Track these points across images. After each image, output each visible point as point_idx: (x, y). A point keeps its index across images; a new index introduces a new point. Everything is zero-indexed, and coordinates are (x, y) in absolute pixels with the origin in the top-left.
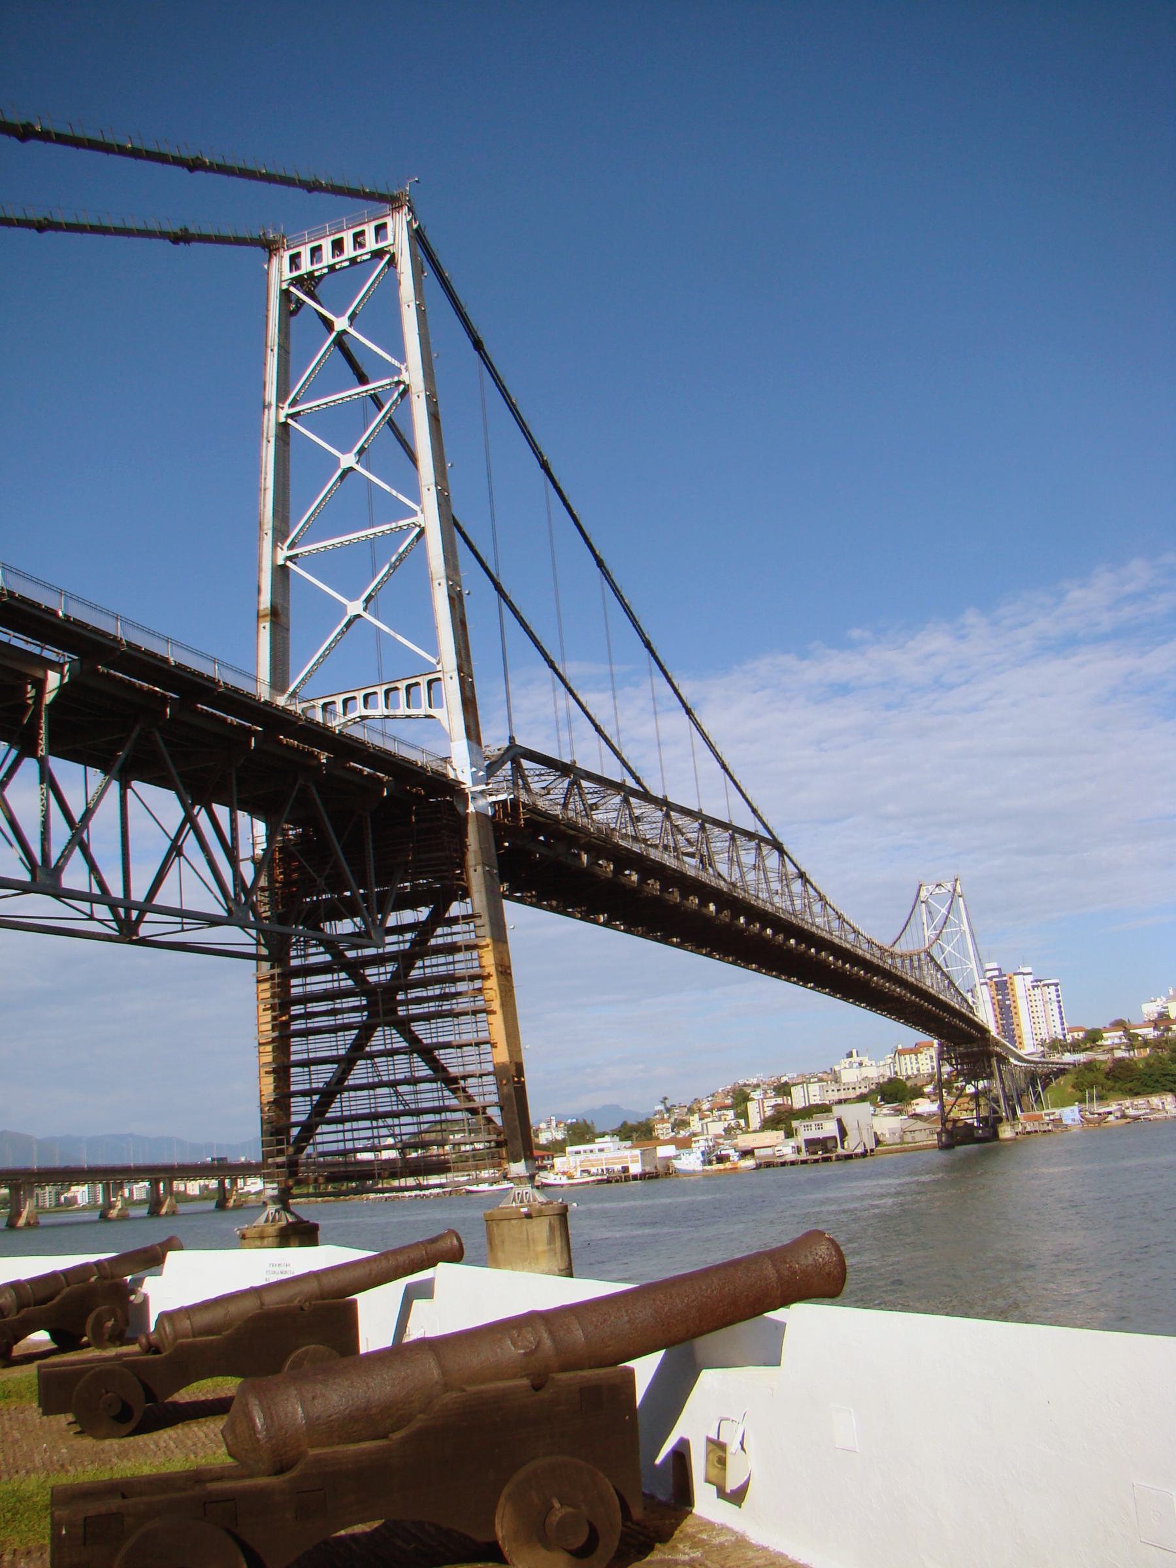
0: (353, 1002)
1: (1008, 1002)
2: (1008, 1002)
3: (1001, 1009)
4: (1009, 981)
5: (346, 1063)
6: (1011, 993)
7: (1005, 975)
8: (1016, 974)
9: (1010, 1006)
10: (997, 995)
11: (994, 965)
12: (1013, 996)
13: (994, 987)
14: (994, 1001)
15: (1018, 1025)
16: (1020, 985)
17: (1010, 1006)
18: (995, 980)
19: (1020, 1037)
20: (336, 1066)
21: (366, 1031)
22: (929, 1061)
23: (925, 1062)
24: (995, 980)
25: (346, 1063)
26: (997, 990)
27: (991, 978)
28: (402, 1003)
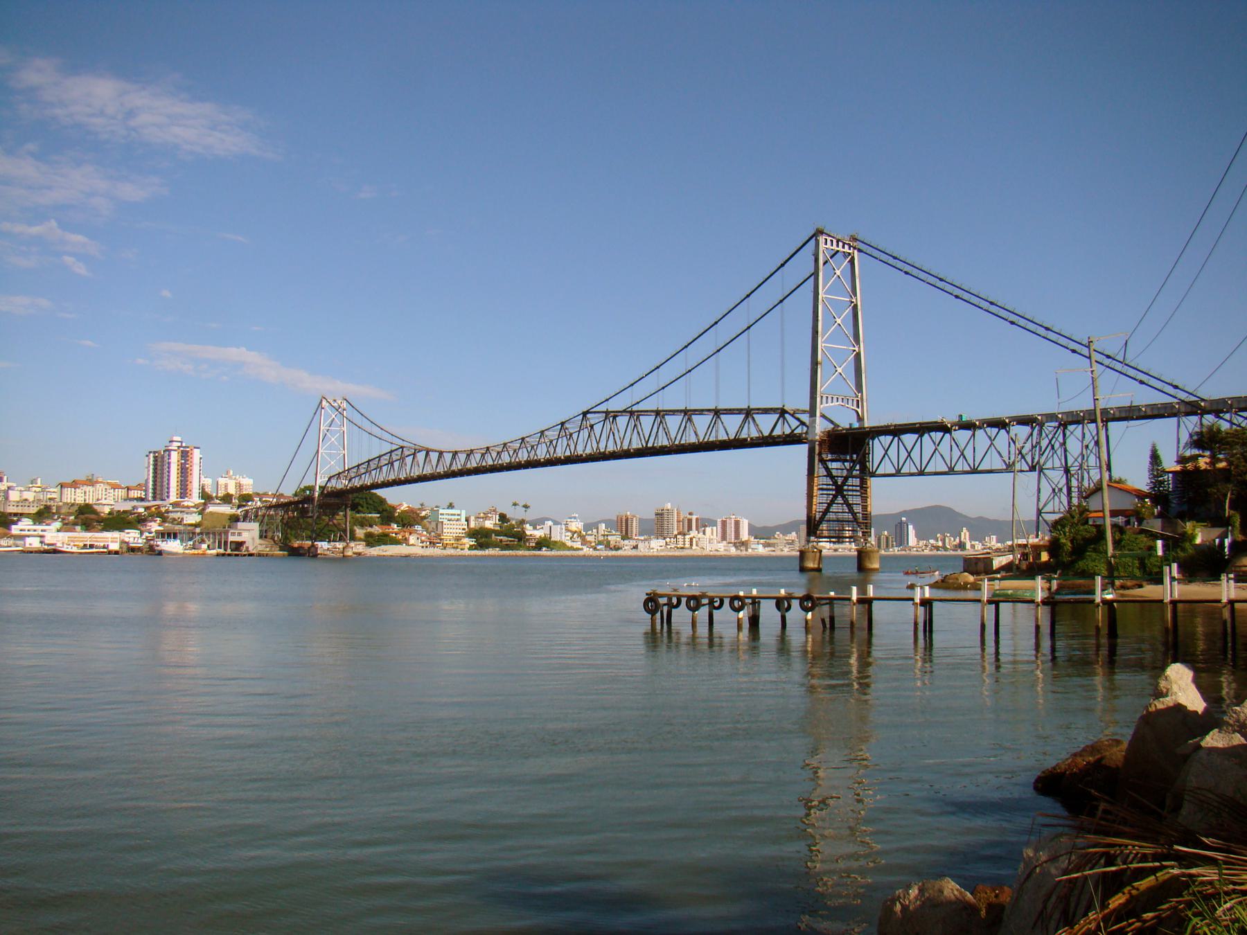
0: (831, 487)
1: (187, 466)
2: (187, 466)
3: (182, 469)
4: (190, 452)
5: (830, 505)
6: (190, 460)
7: (188, 447)
8: (195, 448)
9: (188, 468)
10: (182, 459)
11: (179, 439)
12: (191, 462)
13: (180, 453)
14: (179, 463)
15: (191, 482)
16: (197, 454)
17: (188, 468)
18: (182, 449)
19: (190, 491)
20: (826, 505)
21: (835, 497)
22: (83, 495)
23: (80, 495)
24: (182, 449)
25: (830, 505)
26: (182, 456)
27: (178, 447)
28: (846, 490)
